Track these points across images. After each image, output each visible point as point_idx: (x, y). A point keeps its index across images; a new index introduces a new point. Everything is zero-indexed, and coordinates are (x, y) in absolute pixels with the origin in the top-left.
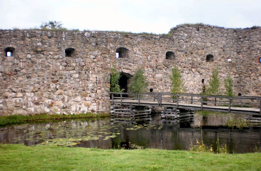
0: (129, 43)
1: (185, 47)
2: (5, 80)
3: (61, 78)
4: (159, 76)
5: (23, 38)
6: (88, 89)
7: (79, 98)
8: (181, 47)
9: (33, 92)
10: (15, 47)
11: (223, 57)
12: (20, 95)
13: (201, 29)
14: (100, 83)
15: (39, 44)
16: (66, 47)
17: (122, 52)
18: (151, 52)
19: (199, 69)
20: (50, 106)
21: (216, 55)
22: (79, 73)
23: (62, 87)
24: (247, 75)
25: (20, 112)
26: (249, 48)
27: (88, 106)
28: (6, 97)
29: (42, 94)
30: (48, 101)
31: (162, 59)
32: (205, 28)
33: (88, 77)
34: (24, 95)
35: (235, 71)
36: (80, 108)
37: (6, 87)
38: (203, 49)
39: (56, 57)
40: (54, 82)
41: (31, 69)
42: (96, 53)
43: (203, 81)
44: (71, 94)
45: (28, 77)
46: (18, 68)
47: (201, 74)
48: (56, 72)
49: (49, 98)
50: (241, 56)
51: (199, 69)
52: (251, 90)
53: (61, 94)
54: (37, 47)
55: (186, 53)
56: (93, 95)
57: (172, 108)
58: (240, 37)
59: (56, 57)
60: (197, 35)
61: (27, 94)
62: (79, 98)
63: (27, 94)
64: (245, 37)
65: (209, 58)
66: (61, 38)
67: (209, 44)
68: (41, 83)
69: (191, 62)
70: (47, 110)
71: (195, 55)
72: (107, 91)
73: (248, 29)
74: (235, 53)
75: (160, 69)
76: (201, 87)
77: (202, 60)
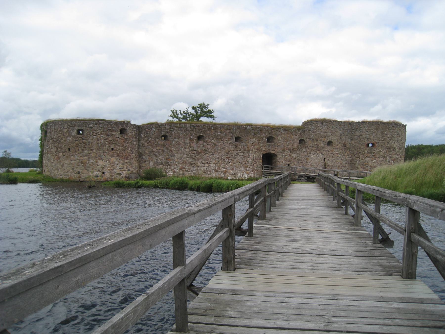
0: (275, 134)
1: (312, 135)
2: (198, 155)
3: (232, 155)
4: (294, 155)
5: (209, 130)
6: (248, 163)
7: (242, 169)
8: (310, 136)
9: (214, 163)
10: (204, 135)
11: (340, 143)
12: (207, 165)
13: (324, 123)
14: (256, 159)
15: (219, 134)
16: (236, 136)
18: (289, 139)
19: (322, 151)
20: (225, 173)
21: (335, 141)
22: (243, 153)
23: (232, 161)
24: (357, 156)
25: (206, 176)
26: (359, 137)
27: (248, 174)
28: (198, 167)
29: (220, 165)
30: (224, 170)
32: (327, 122)
33: (249, 155)
34: (209, 166)
35: (349, 152)
36: (243, 175)
37: (198, 160)
38: (325, 137)
39: (229, 142)
40: (227, 158)
41: (214, 150)
42: (254, 140)
43: (324, 159)
44: (237, 166)
45: (212, 154)
46: (206, 149)
47: (323, 155)
48: (229, 151)
49: (224, 168)
50: (353, 142)
51: (322, 151)
52: (359, 167)
53: (231, 166)
54: (218, 135)
55: (313, 140)
56: (251, 167)
57: (302, 176)
58: (353, 128)
59: (229, 142)
60: (321, 127)
61: (211, 165)
63: (211, 165)
64: (357, 129)
65: (330, 143)
66: (233, 130)
67: (330, 134)
68: (220, 158)
69: (316, 146)
70: (223, 176)
71: (320, 142)
72: (260, 165)
73: (359, 122)
74: (349, 140)
75: (295, 151)
76: (323, 164)
77: (325, 145)
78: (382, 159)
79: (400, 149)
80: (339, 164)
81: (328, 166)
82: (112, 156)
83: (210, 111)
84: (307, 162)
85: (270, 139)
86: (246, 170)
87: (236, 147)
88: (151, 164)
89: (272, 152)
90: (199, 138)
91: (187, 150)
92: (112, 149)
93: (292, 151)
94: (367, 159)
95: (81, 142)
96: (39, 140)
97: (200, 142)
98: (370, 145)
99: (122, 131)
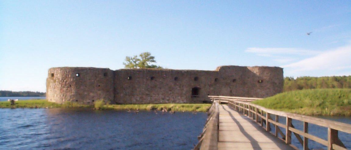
4: (212, 89)
5: (158, 73)
7: (179, 98)
12: (157, 95)
17: (196, 79)
31: (213, 82)
50: (249, 80)
53: (172, 96)
62: (179, 98)
78: (268, 90)
79: (280, 83)
82: (99, 90)
83: (153, 58)
85: (196, 79)
86: (182, 98)
87: (175, 84)
88: (122, 95)
89: (198, 87)
90: (152, 78)
91: (144, 86)
92: (99, 86)
93: (210, 86)
94: (259, 90)
95: (79, 81)
97: (153, 81)
98: (260, 81)
99: (105, 75)
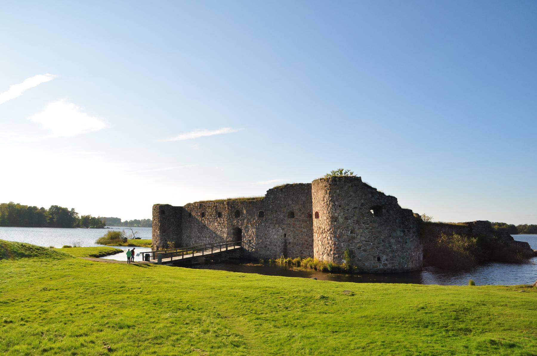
1: (271, 207)
13: (284, 190)
21: (297, 211)
38: (285, 207)
43: (285, 235)
47: (283, 229)
67: (290, 202)
76: (283, 241)
77: (284, 216)
79: (346, 218)
80: (304, 242)
81: (290, 243)
84: (266, 238)
96: (73, 209)
